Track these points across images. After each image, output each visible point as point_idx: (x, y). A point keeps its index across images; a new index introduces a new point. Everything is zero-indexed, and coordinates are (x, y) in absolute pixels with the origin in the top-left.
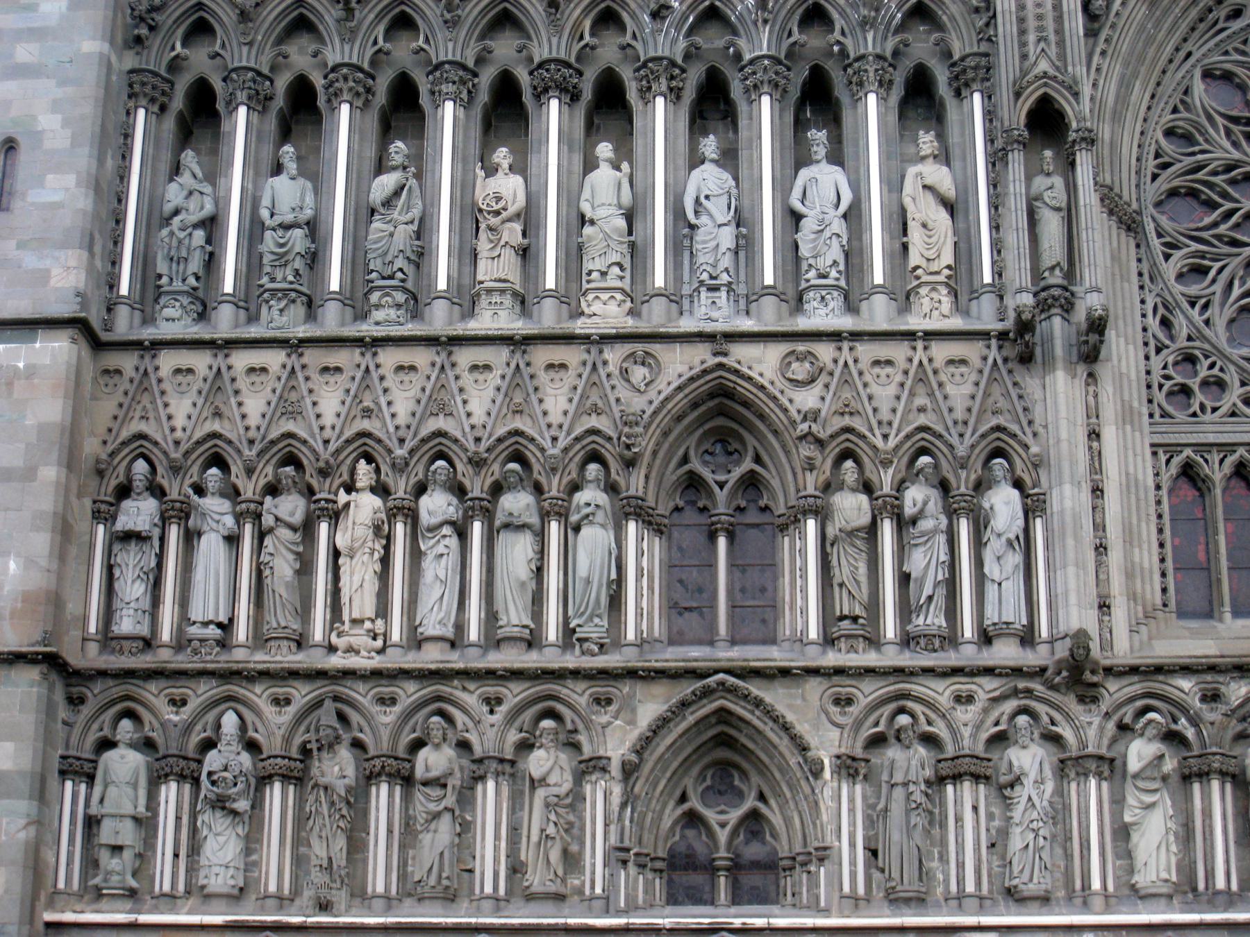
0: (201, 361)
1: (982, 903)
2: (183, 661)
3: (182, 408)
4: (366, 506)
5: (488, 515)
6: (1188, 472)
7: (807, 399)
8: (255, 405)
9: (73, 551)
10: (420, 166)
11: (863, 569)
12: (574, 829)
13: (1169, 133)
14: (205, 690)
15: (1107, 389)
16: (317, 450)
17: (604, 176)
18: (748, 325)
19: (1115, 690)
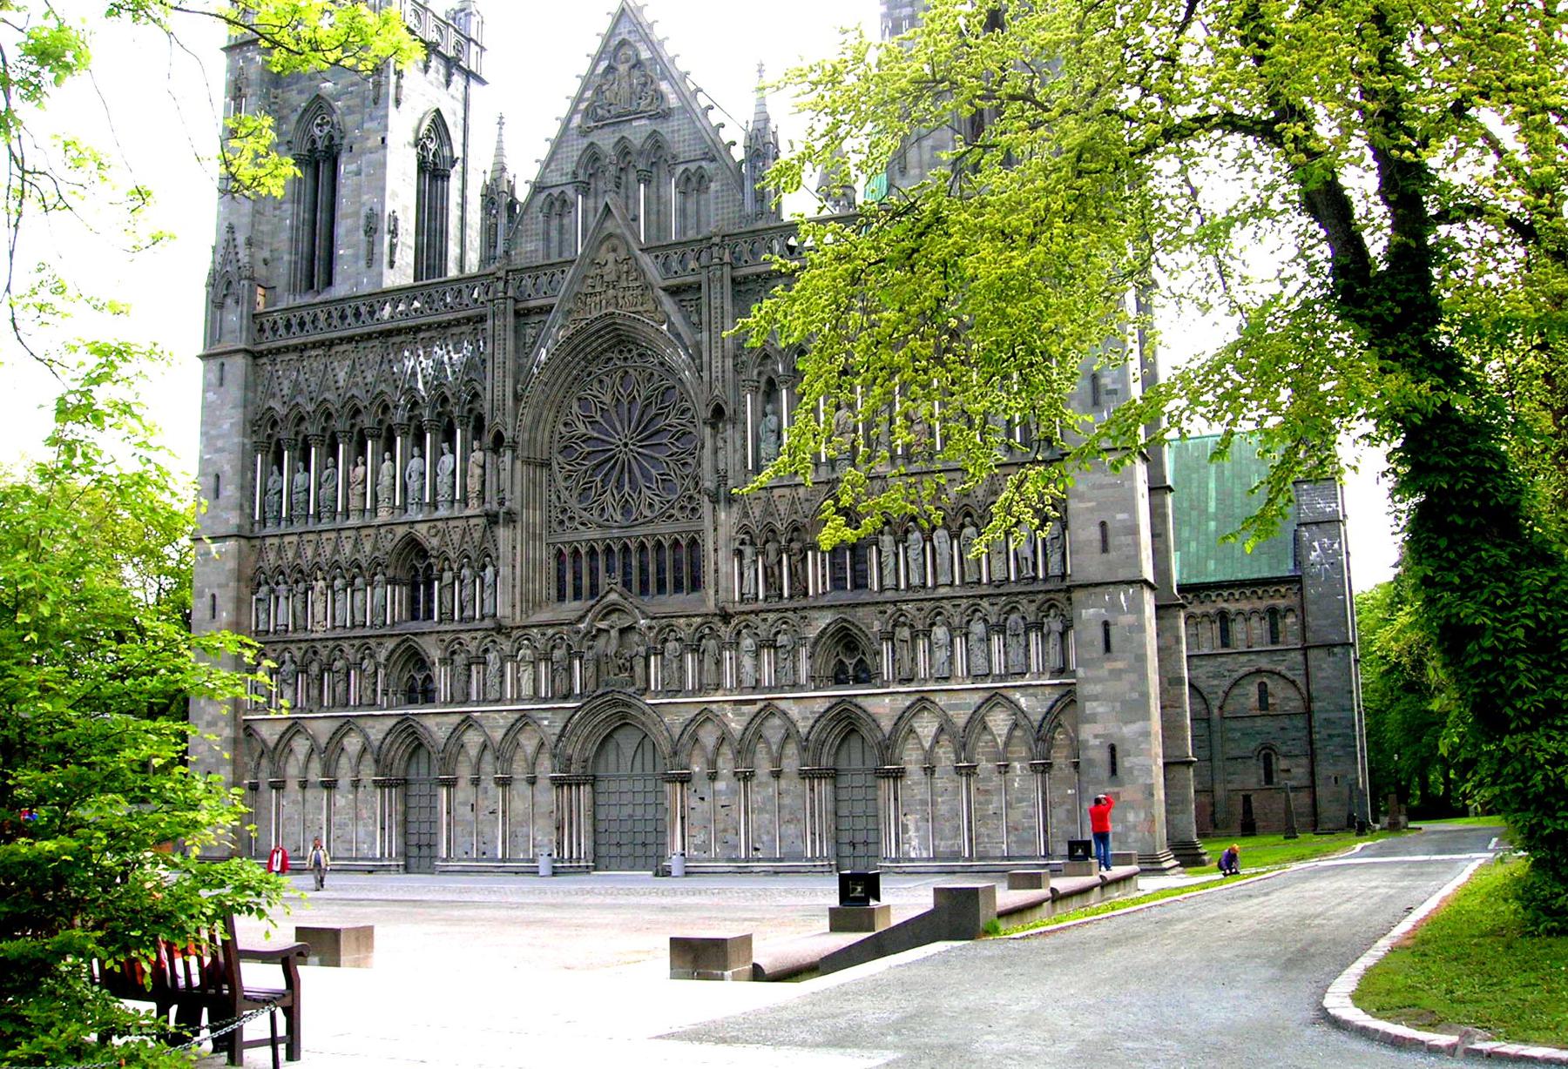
0: (276, 541)
1: (478, 703)
2: (275, 638)
3: (272, 556)
4: (321, 583)
5: (352, 584)
6: (560, 553)
7: (435, 542)
8: (290, 554)
9: (245, 609)
10: (336, 467)
11: (449, 597)
12: (375, 683)
13: (566, 424)
14: (280, 647)
15: (519, 531)
16: (306, 569)
17: (388, 463)
18: (420, 517)
19: (515, 634)
